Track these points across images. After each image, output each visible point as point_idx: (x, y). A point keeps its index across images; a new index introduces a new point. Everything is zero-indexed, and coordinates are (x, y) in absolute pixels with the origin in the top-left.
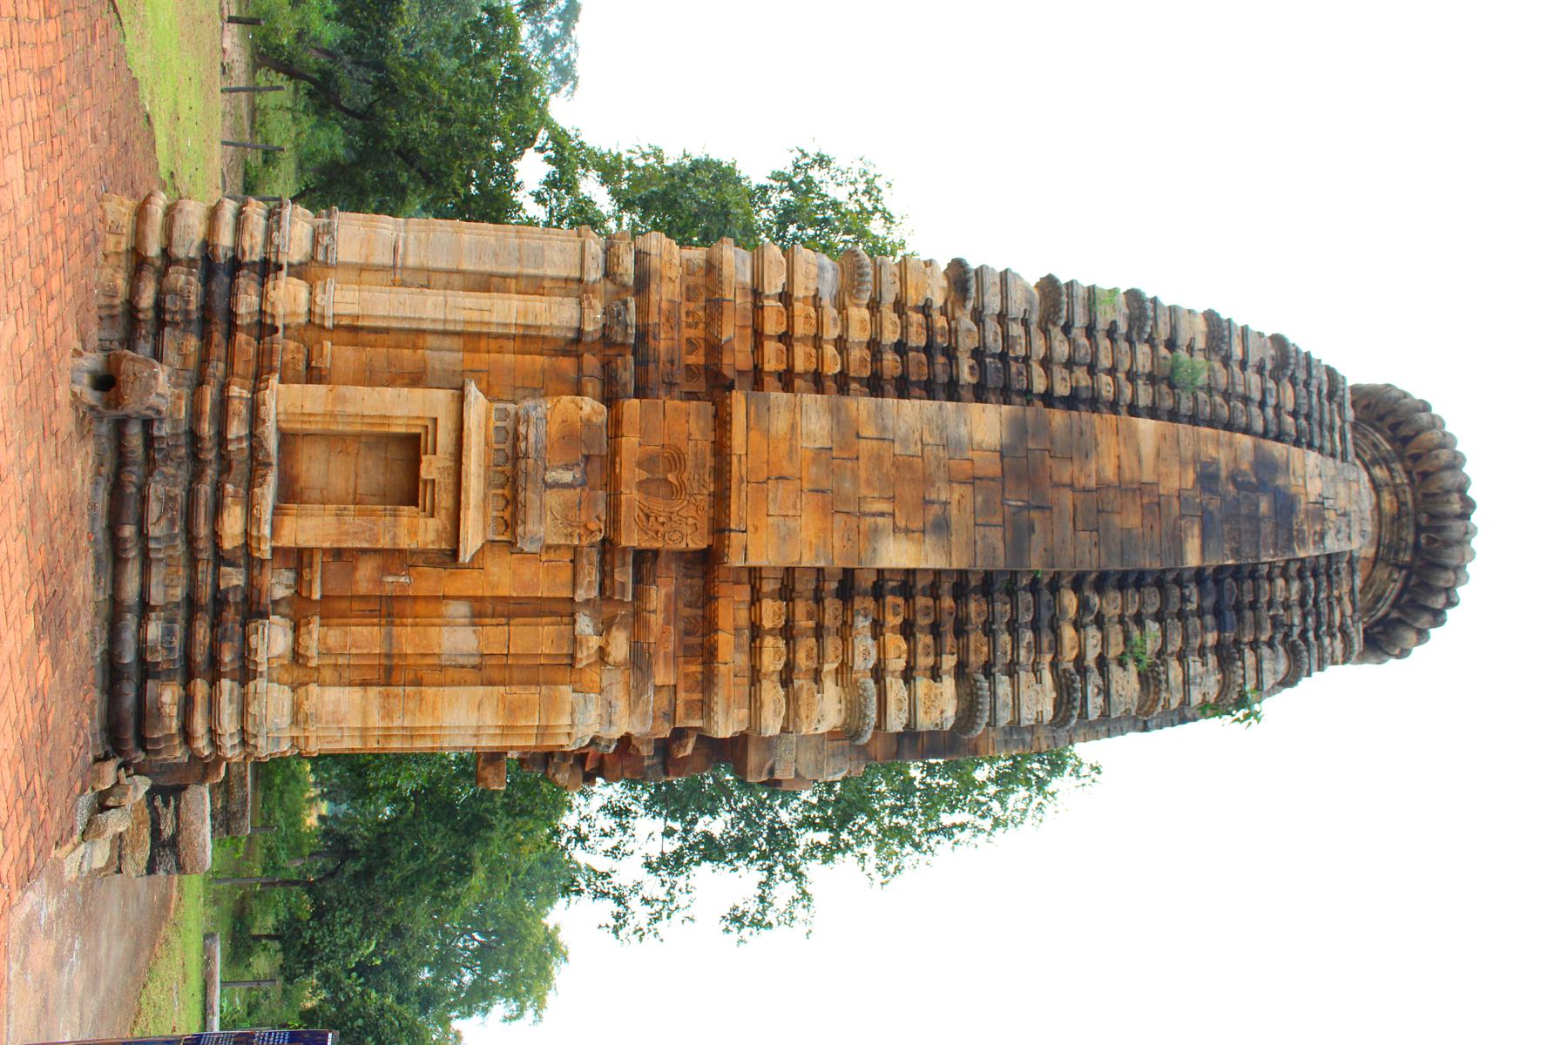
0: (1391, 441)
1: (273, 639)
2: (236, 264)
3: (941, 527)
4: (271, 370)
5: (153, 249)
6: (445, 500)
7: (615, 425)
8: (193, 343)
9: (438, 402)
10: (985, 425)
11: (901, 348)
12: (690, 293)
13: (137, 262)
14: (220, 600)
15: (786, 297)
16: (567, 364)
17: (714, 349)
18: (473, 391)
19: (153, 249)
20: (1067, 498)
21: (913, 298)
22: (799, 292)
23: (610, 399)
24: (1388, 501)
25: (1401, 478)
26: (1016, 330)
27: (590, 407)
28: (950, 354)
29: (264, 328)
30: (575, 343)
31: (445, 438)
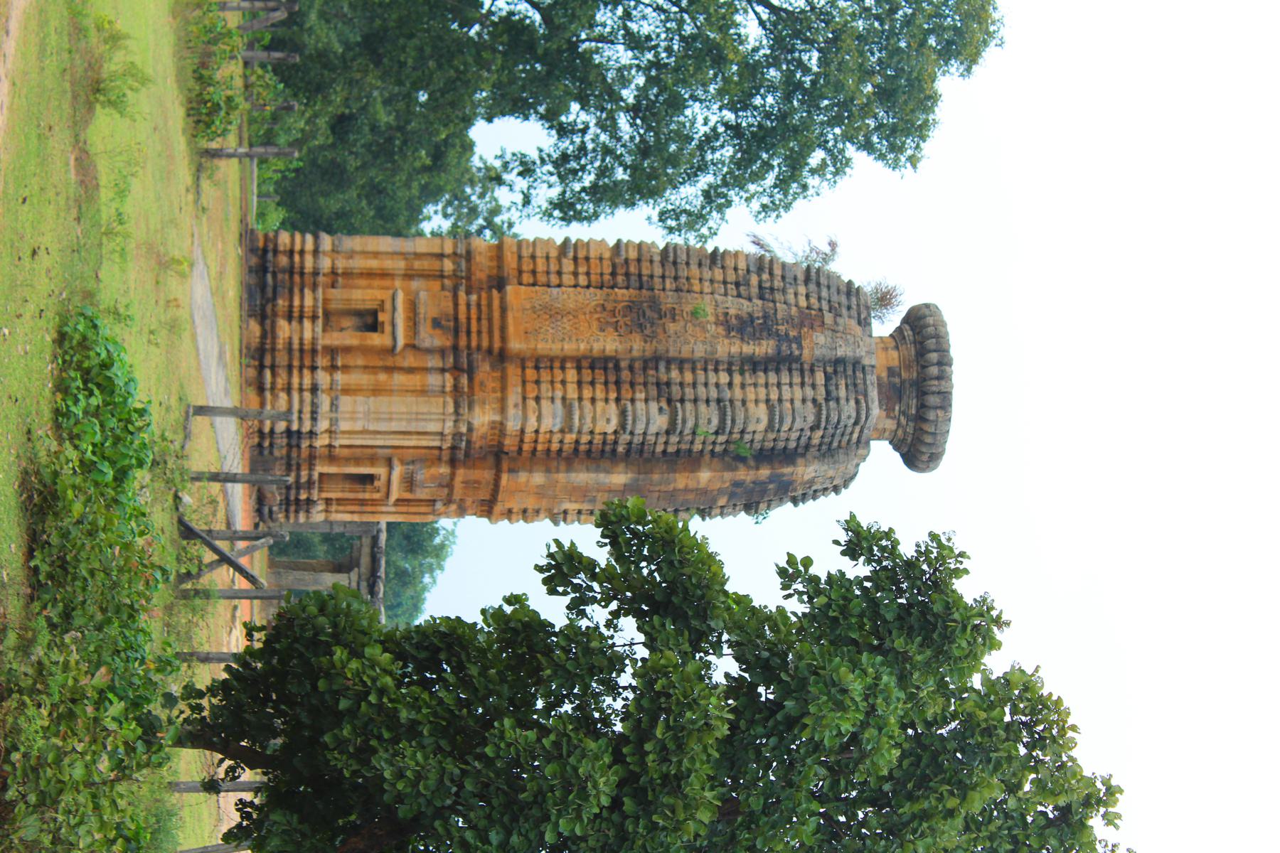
0: (917, 411)
1: (321, 507)
2: (299, 432)
3: (593, 500)
4: (315, 458)
5: (267, 430)
6: (384, 490)
7: (453, 475)
8: (284, 451)
9: (380, 471)
10: (619, 478)
11: (590, 442)
12: (492, 428)
13: (261, 433)
14: (297, 501)
15: (537, 432)
16: (436, 452)
17: (501, 445)
18: (396, 462)
19: (267, 430)
20: (657, 494)
21: (597, 431)
22: (542, 430)
23: (453, 462)
24: (900, 432)
25: (910, 430)
26: (651, 439)
27: (444, 470)
28: (616, 442)
29: (311, 446)
30: (440, 448)
31: (384, 478)
